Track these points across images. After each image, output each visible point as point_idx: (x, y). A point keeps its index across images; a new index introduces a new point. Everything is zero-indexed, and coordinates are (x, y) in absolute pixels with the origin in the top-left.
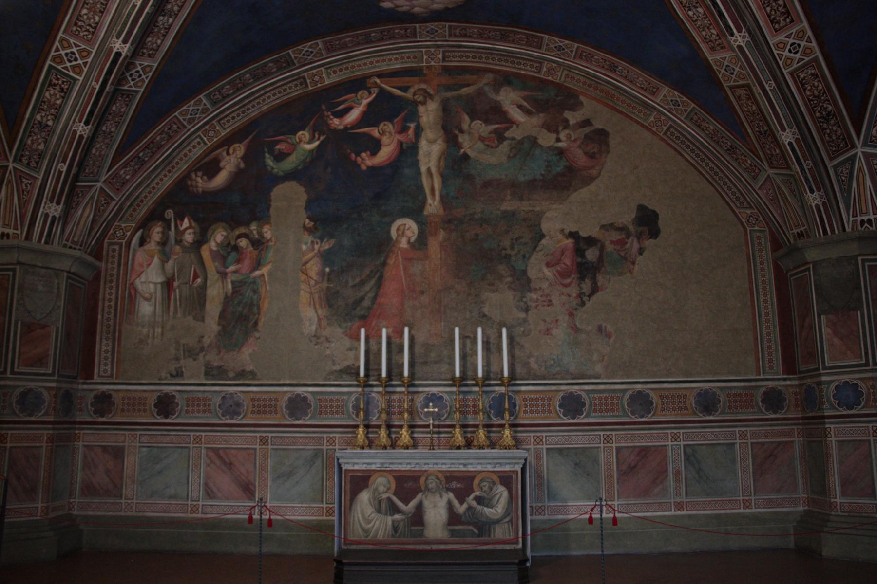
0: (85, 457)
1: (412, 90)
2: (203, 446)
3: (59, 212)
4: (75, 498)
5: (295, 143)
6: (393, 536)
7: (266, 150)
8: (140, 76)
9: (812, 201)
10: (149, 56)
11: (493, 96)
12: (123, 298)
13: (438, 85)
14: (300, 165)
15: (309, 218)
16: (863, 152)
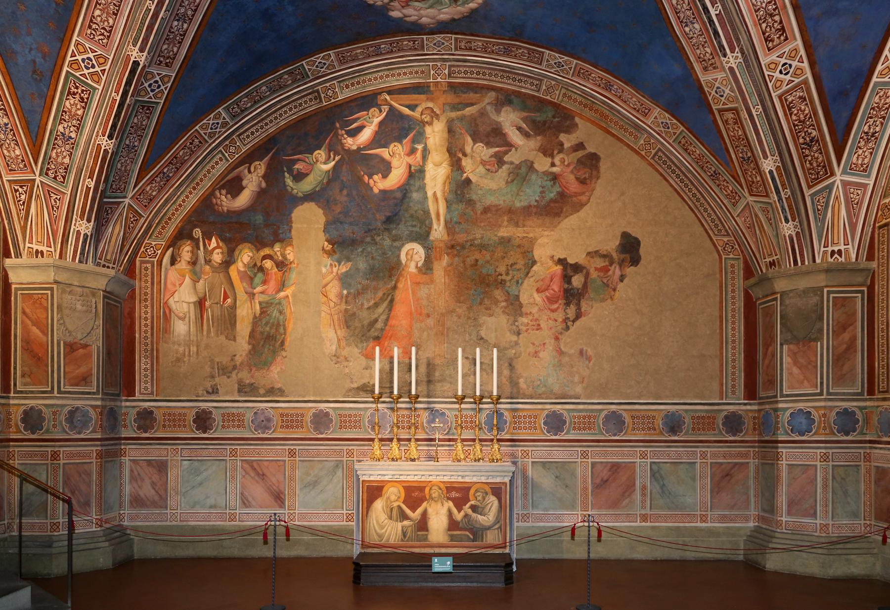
0: (132, 471)
1: (419, 109)
2: (238, 458)
3: (90, 230)
4: (125, 510)
5: (312, 163)
6: (402, 540)
7: (285, 169)
8: (159, 87)
9: (786, 231)
10: (167, 65)
11: (494, 116)
12: (158, 318)
13: (444, 104)
15: (327, 240)
16: (841, 180)
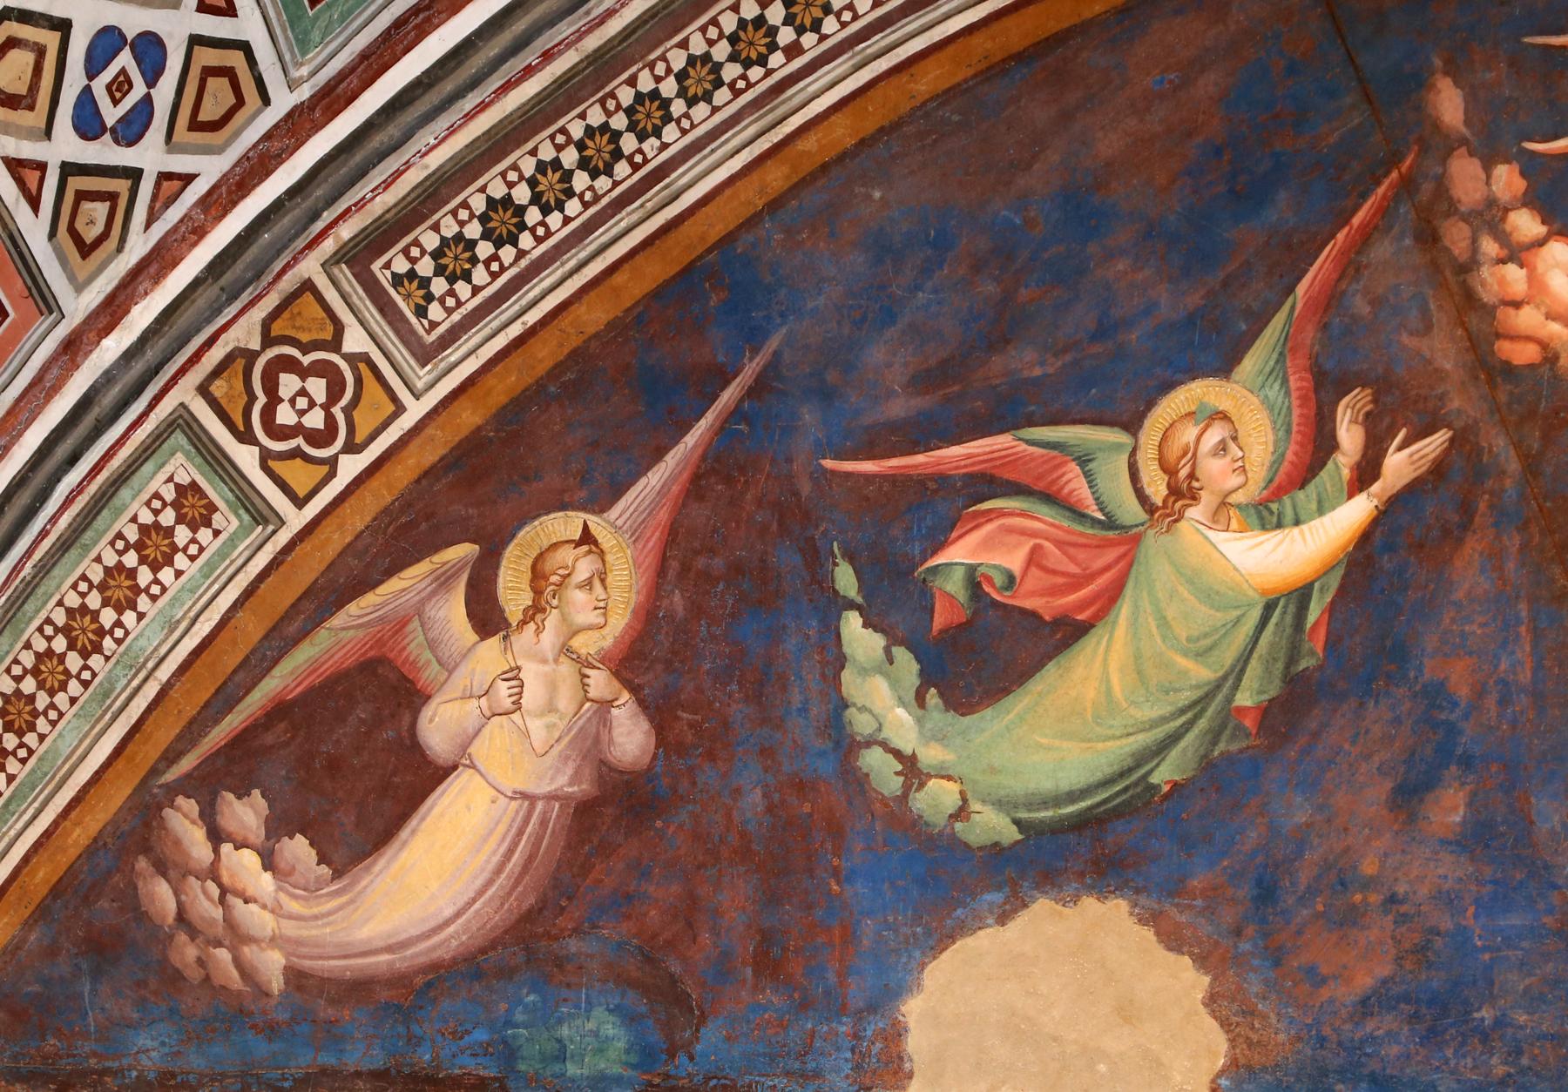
5: (1130, 512)
7: (846, 580)
14: (1161, 749)
